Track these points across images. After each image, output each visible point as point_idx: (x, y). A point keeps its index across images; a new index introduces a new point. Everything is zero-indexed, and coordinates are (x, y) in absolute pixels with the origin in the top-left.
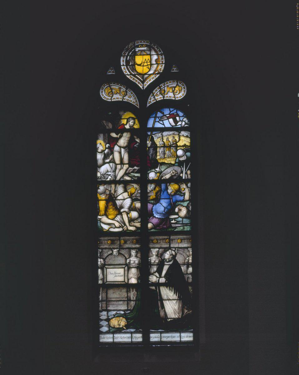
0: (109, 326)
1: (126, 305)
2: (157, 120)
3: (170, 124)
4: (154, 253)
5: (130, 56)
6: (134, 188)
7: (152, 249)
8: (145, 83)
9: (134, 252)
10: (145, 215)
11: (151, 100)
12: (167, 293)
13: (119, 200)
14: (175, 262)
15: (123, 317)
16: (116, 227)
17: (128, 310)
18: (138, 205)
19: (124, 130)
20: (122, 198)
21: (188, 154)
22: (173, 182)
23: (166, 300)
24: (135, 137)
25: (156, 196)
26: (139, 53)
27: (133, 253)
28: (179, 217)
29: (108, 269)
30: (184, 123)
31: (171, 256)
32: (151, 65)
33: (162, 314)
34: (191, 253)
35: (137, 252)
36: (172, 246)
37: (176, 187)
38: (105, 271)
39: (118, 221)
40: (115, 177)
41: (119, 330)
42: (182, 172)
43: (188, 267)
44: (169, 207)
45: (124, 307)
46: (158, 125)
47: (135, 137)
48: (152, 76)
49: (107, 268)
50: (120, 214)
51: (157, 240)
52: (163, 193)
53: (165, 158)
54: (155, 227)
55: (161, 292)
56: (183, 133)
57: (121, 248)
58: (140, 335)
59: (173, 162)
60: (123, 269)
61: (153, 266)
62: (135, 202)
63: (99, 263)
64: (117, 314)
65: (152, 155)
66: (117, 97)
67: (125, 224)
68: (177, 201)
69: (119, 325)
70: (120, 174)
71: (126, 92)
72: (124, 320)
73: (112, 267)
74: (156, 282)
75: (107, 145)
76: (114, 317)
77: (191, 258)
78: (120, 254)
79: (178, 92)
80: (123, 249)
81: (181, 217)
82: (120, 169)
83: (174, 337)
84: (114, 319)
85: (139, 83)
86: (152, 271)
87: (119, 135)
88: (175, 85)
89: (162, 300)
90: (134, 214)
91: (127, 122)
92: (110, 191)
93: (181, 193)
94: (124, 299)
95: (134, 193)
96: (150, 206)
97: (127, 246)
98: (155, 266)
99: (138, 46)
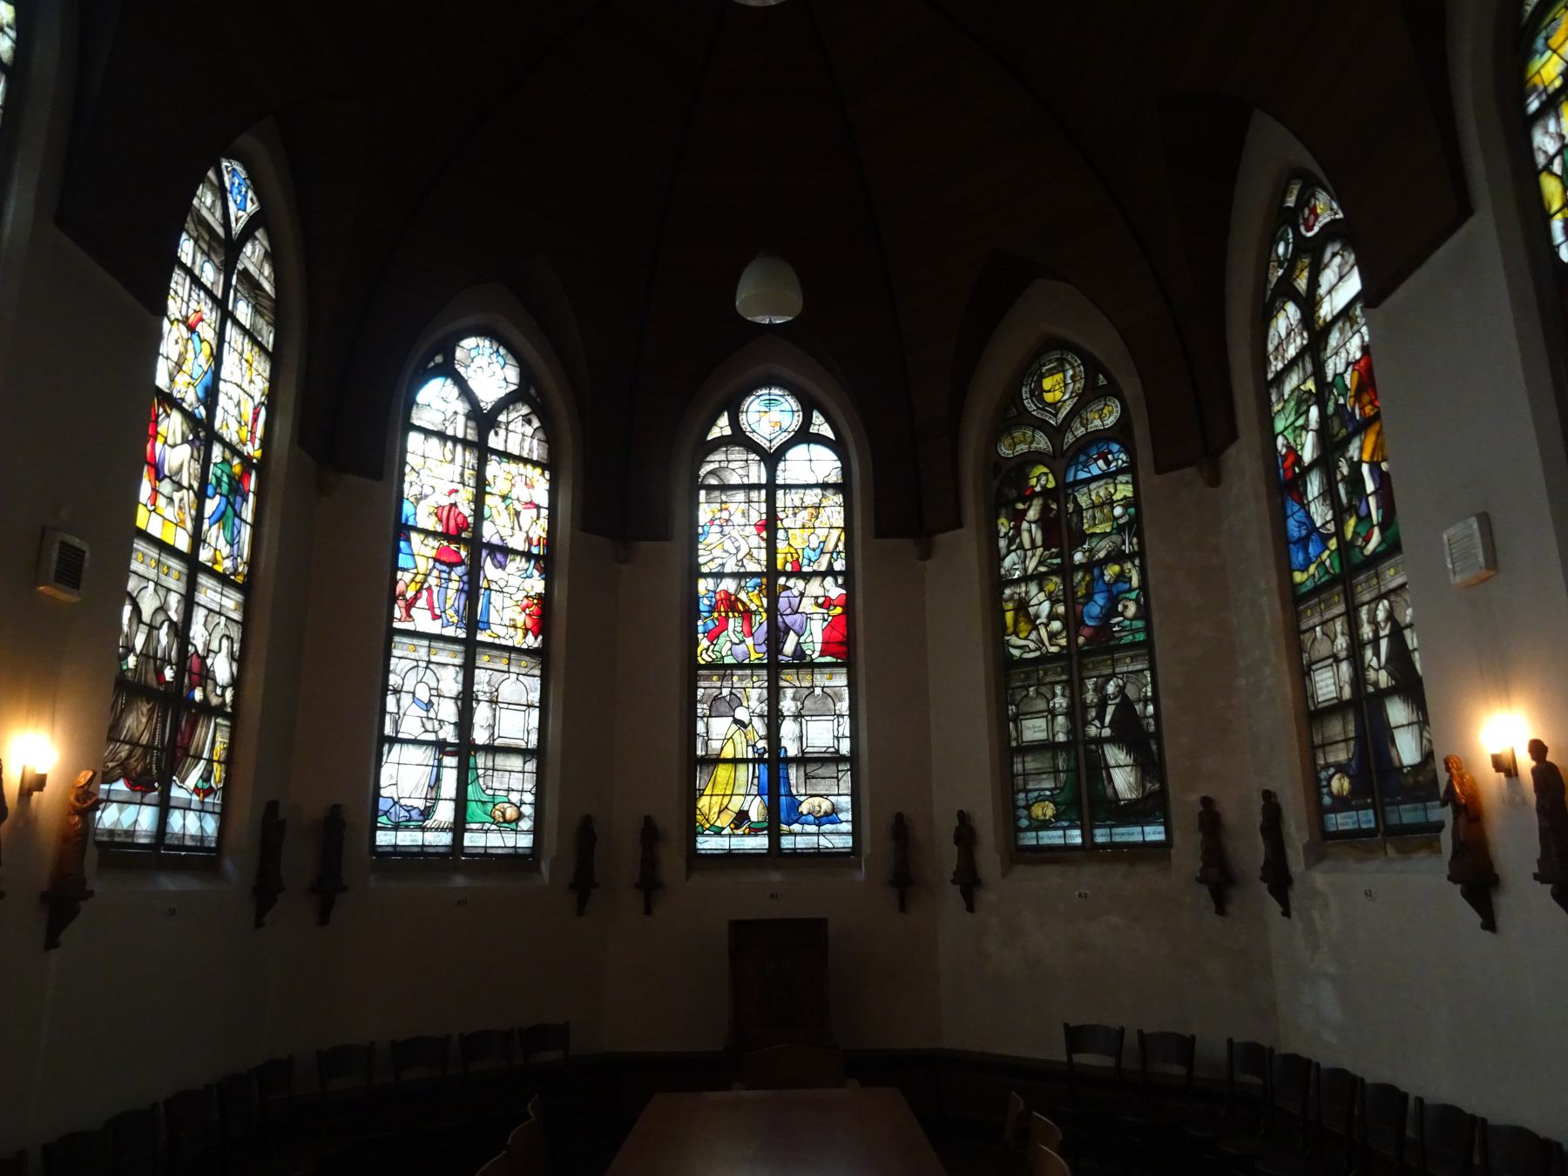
0: (1029, 817)
1: (1053, 781)
2: (1080, 467)
3: (1100, 469)
4: (1090, 687)
5: (1035, 382)
6: (1054, 584)
7: (1086, 681)
8: (1059, 416)
9: (1059, 688)
10: (1073, 622)
11: (1070, 439)
12: (1115, 755)
13: (1033, 606)
14: (1125, 697)
15: (1051, 802)
16: (1031, 651)
17: (1056, 788)
18: (1061, 609)
19: (1035, 495)
20: (1037, 602)
21: (1132, 510)
22: (1111, 562)
23: (1114, 767)
24: (1050, 502)
25: (1086, 589)
26: (1047, 374)
27: (1058, 689)
28: (1125, 618)
29: (1023, 722)
30: (1120, 462)
31: (1118, 689)
32: (1066, 385)
33: (1110, 791)
34: (1149, 679)
35: (1063, 688)
36: (1117, 670)
37: (1116, 568)
39: (1032, 641)
40: (1025, 570)
41: (1045, 825)
42: (1124, 543)
43: (1146, 706)
44: (1108, 605)
45: (1049, 784)
46: (1082, 475)
47: (1050, 502)
48: (1068, 403)
49: (1021, 720)
50: (1036, 628)
51: (1093, 663)
52: (1098, 582)
53: (1096, 525)
54: (1089, 641)
55: (1106, 752)
56: (1121, 478)
57: (1040, 684)
58: (1077, 832)
59: (1108, 530)
60: (1045, 719)
61: (1090, 710)
62: (1056, 606)
63: (1010, 712)
64: (1040, 795)
65: (1076, 524)
66: (1022, 448)
67: (1044, 644)
68: (1120, 593)
69: (1044, 815)
70: (1031, 565)
71: (1033, 436)
72: (1051, 805)
73: (1029, 716)
75: (1012, 524)
76: (1036, 802)
77: (1149, 689)
78: (1038, 693)
79: (1108, 415)
80: (1044, 685)
81: (1128, 619)
82: (1031, 558)
83: (1131, 834)
84: (1036, 805)
85: (1050, 418)
86: (1090, 718)
87: (1027, 505)
88: (1102, 406)
89: (1108, 767)
90: (1056, 625)
91: (1038, 481)
92: (1020, 594)
93: (1125, 577)
94: (1050, 770)
95: (1053, 592)
96: (1079, 608)
97: (1048, 679)
98: (1094, 709)
99: (1045, 365)
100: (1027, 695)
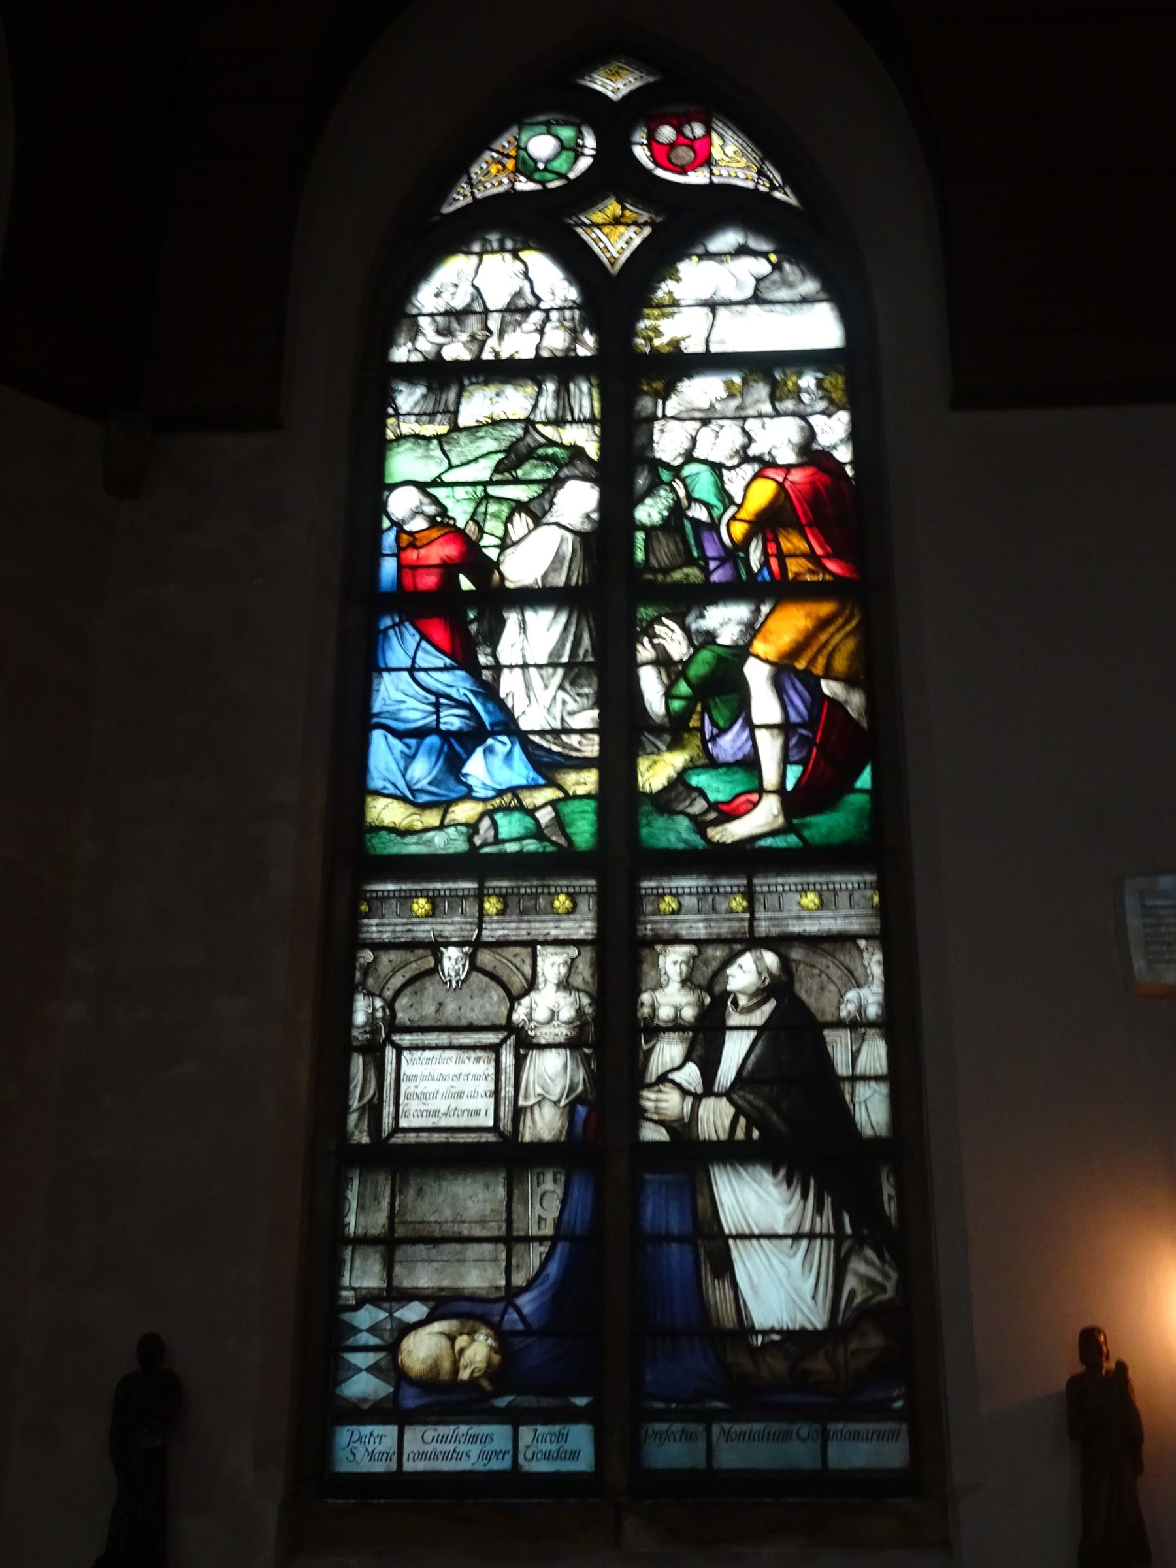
38: (390, 1066)
63: (360, 1018)
73: (431, 1038)
74: (682, 1118)
78: (474, 967)
100: (434, 971)
